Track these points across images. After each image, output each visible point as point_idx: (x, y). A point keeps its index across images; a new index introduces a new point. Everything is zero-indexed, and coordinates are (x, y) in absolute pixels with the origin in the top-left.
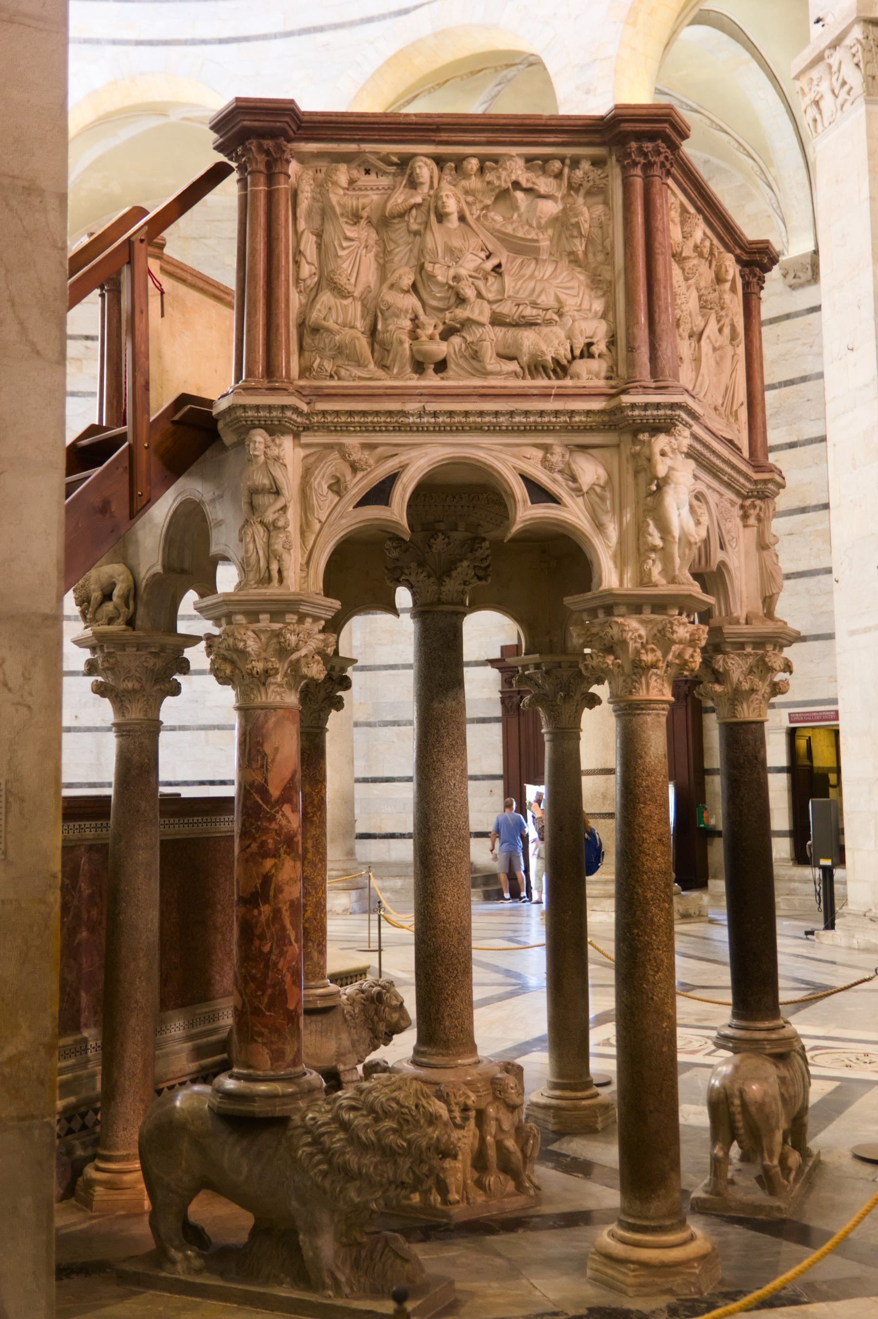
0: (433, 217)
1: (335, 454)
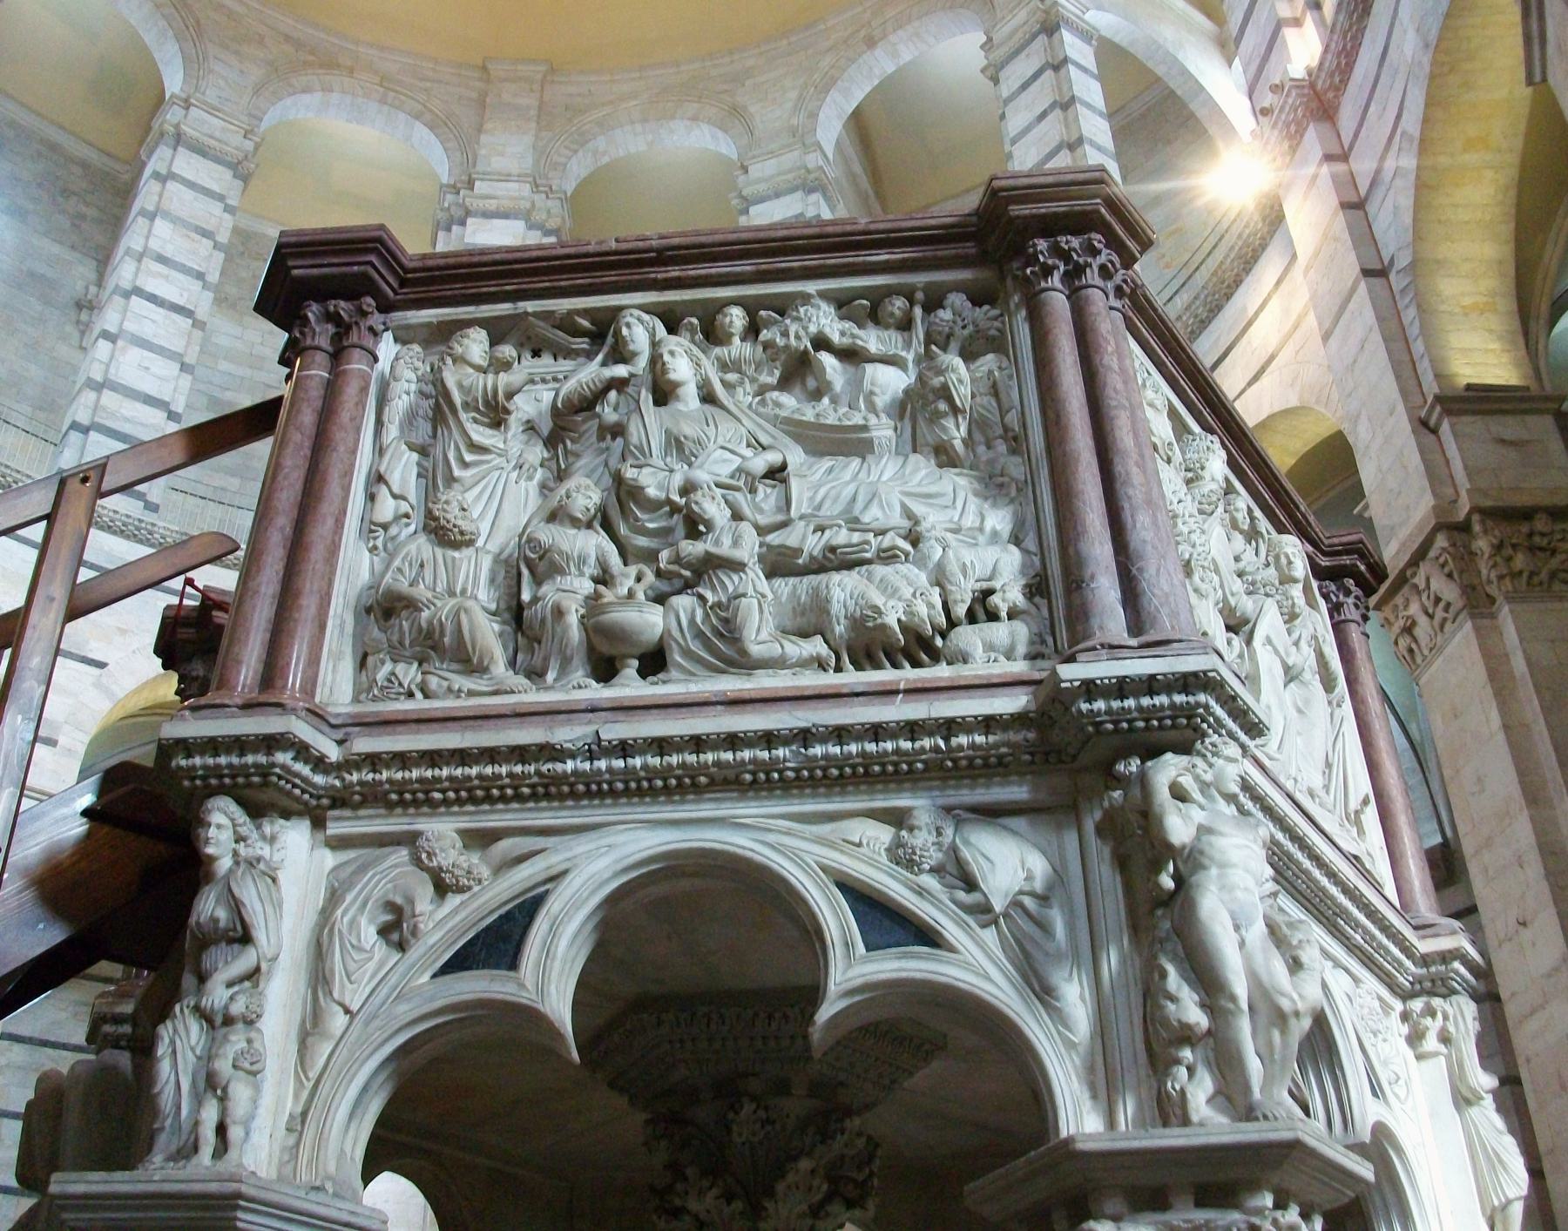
0: (646, 398)
1: (403, 854)
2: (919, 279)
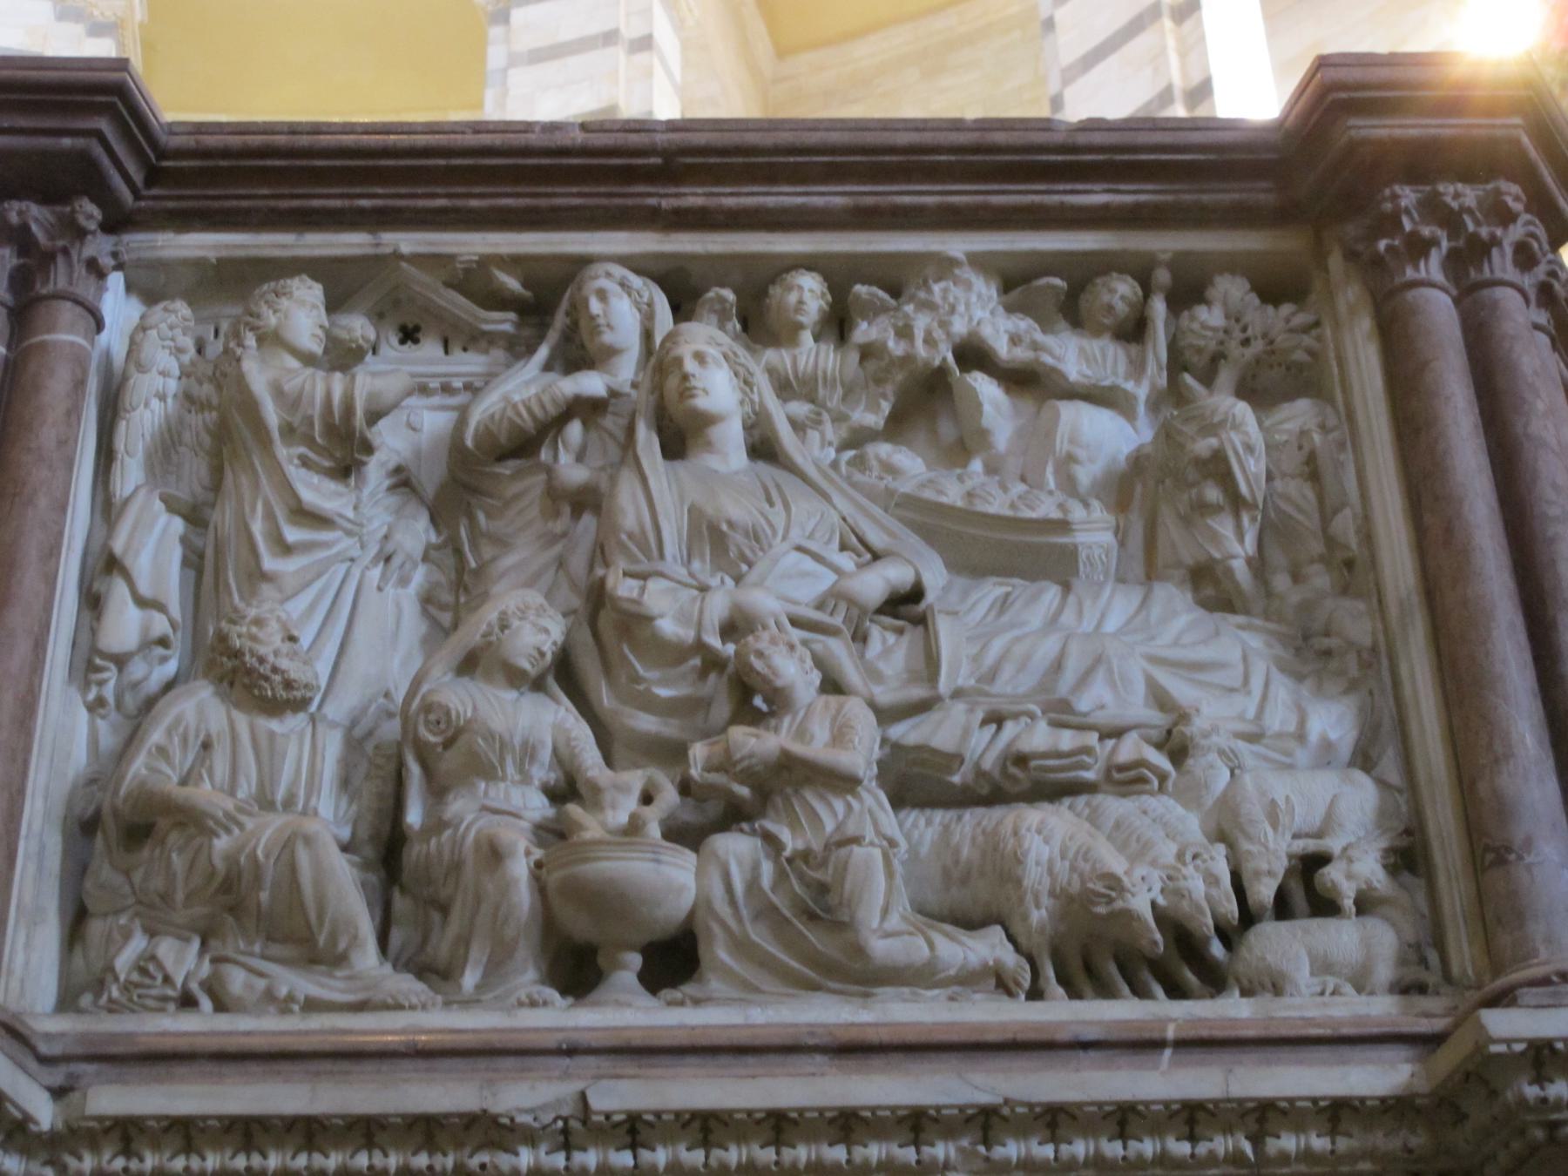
0: (647, 441)
2: (1164, 243)
